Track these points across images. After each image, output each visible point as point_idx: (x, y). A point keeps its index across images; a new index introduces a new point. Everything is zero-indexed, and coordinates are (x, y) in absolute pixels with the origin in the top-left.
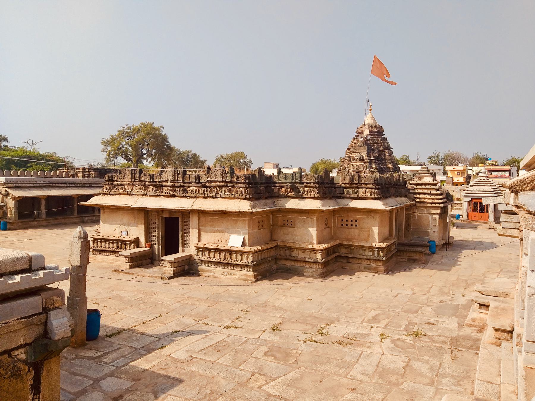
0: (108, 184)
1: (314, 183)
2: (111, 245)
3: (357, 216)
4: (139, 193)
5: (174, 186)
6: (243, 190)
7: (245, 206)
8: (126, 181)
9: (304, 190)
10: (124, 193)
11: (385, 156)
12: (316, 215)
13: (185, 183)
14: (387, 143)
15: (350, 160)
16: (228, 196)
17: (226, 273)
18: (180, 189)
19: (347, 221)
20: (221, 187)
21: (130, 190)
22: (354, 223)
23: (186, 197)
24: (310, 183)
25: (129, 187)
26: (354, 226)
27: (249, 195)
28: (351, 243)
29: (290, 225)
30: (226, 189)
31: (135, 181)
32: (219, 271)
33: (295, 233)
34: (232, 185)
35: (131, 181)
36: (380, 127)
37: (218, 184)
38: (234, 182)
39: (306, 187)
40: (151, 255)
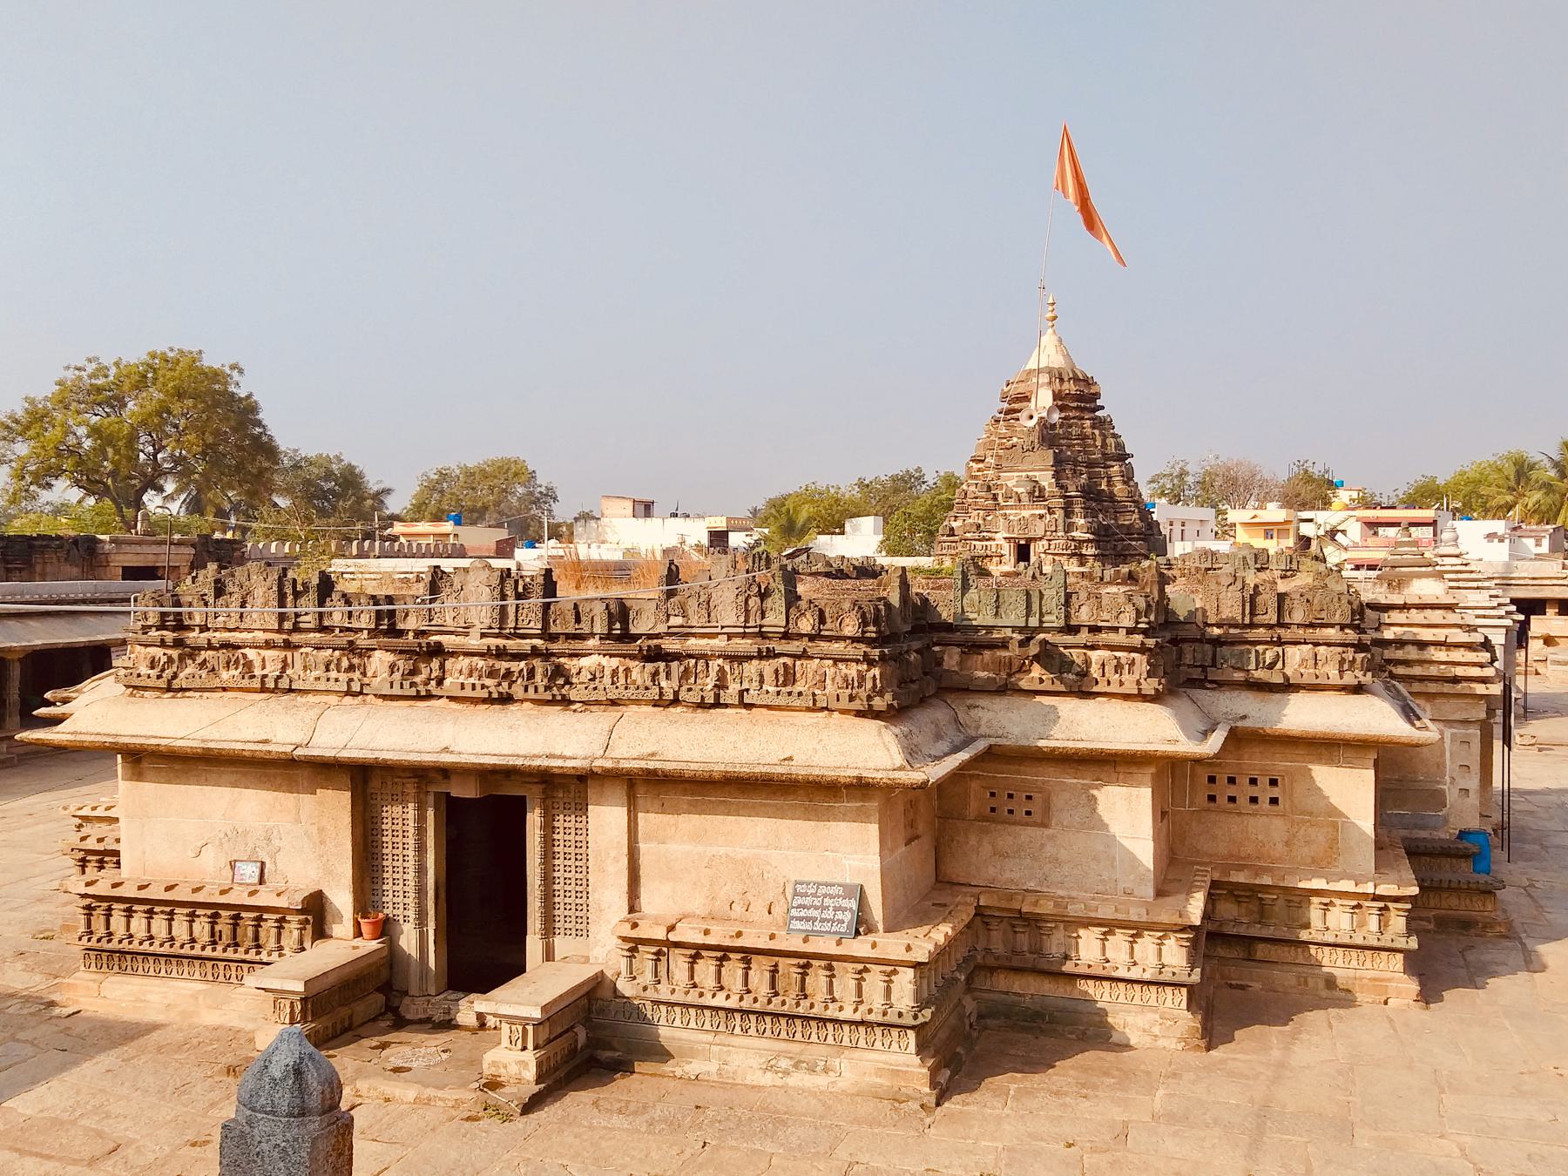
0: (163, 644)
1: (1130, 631)
2: (180, 929)
3: (1280, 763)
4: (322, 686)
5: (501, 654)
6: (852, 671)
7: (873, 750)
8: (250, 630)
9: (1088, 662)
10: (246, 683)
11: (1109, 483)
12: (1153, 770)
13: (553, 638)
14: (1115, 436)
15: (995, 498)
16: (782, 701)
17: (784, 1063)
18: (534, 663)
19: (1232, 781)
20: (738, 659)
21: (272, 670)
22: (1264, 792)
23: (566, 702)
24: (1115, 629)
25: (269, 654)
26: (1264, 803)
27: (881, 694)
28: (1267, 880)
29: (1020, 814)
30: (768, 667)
31: (296, 629)
32: (746, 1058)
33: (1050, 849)
34: (795, 647)
35: (280, 631)
36: (1088, 382)
37: (720, 643)
38: (801, 636)
39: (1093, 648)
40: (385, 973)
